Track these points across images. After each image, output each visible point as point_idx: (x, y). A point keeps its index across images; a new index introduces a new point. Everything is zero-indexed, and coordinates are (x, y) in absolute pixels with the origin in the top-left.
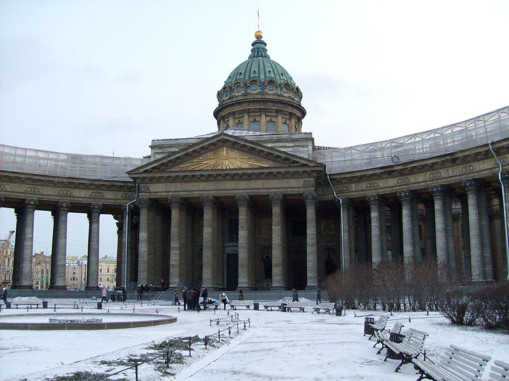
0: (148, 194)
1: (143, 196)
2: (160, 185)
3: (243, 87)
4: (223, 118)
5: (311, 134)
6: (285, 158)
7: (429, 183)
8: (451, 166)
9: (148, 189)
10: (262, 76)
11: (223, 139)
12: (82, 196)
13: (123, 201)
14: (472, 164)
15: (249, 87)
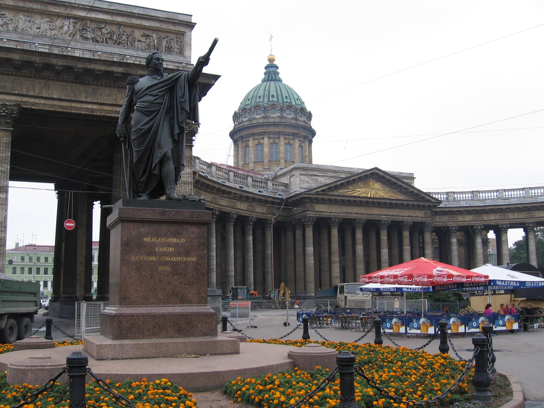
0: (314, 213)
1: (310, 214)
2: (323, 206)
3: (279, 110)
4: (253, 135)
5: (413, 174)
6: (417, 194)
7: (499, 221)
8: (517, 212)
9: (314, 209)
10: (294, 103)
11: (375, 172)
12: (242, 208)
13: (268, 215)
14: (534, 212)
15: (285, 110)
